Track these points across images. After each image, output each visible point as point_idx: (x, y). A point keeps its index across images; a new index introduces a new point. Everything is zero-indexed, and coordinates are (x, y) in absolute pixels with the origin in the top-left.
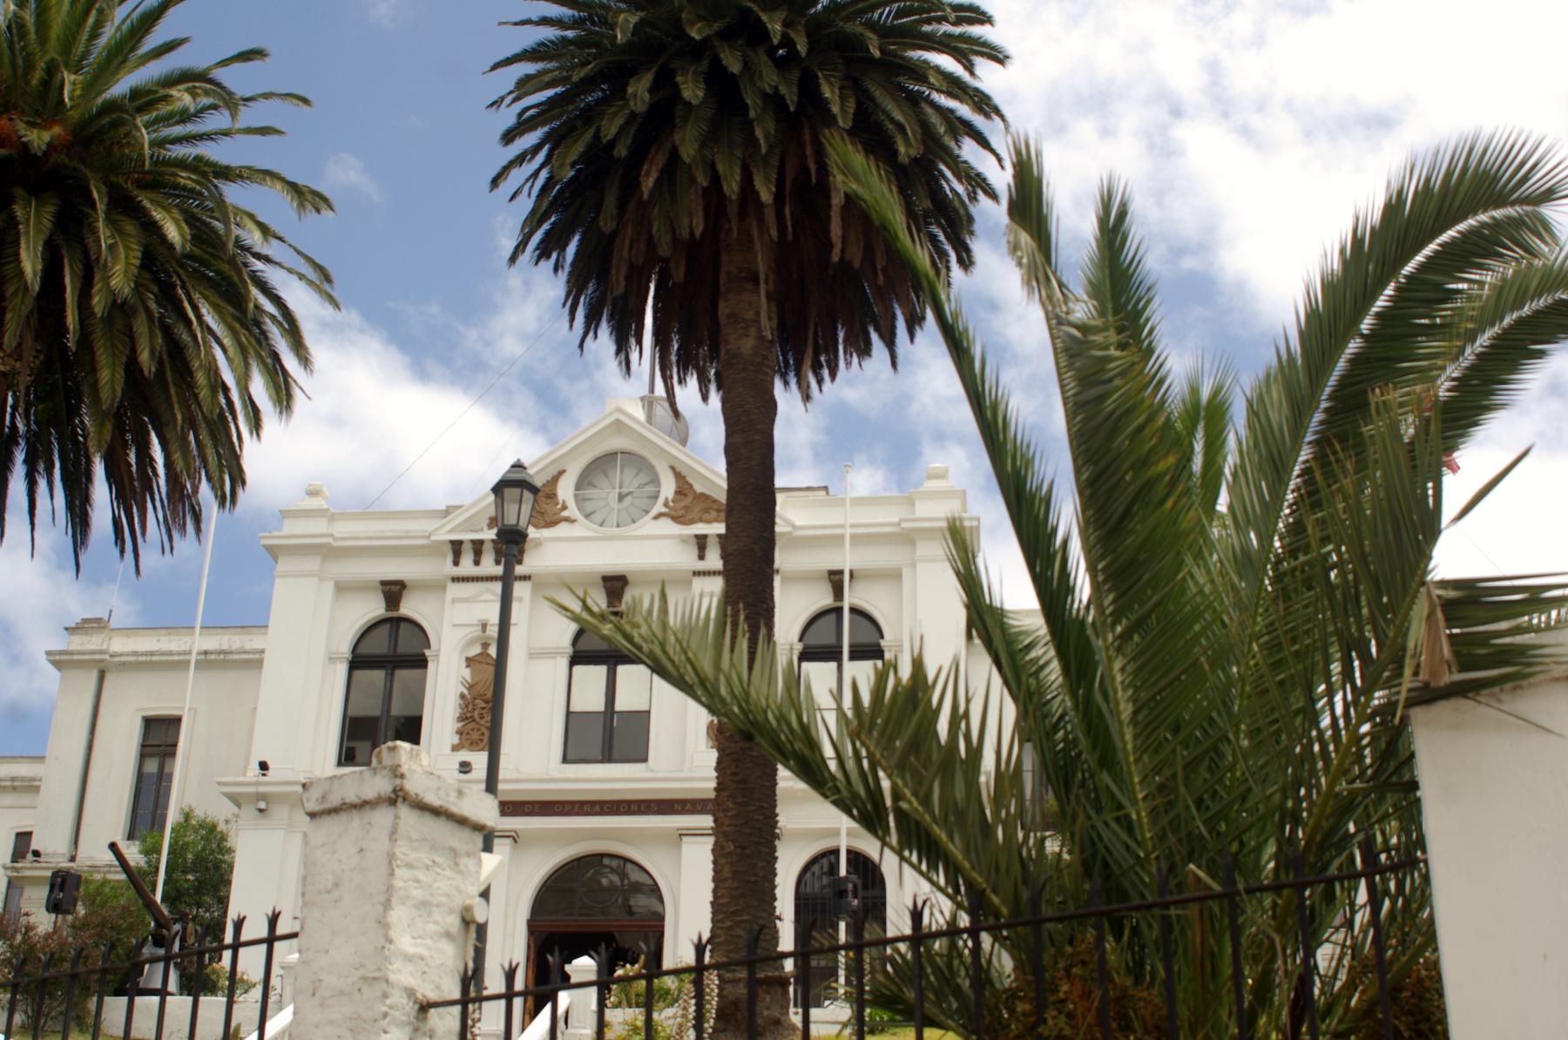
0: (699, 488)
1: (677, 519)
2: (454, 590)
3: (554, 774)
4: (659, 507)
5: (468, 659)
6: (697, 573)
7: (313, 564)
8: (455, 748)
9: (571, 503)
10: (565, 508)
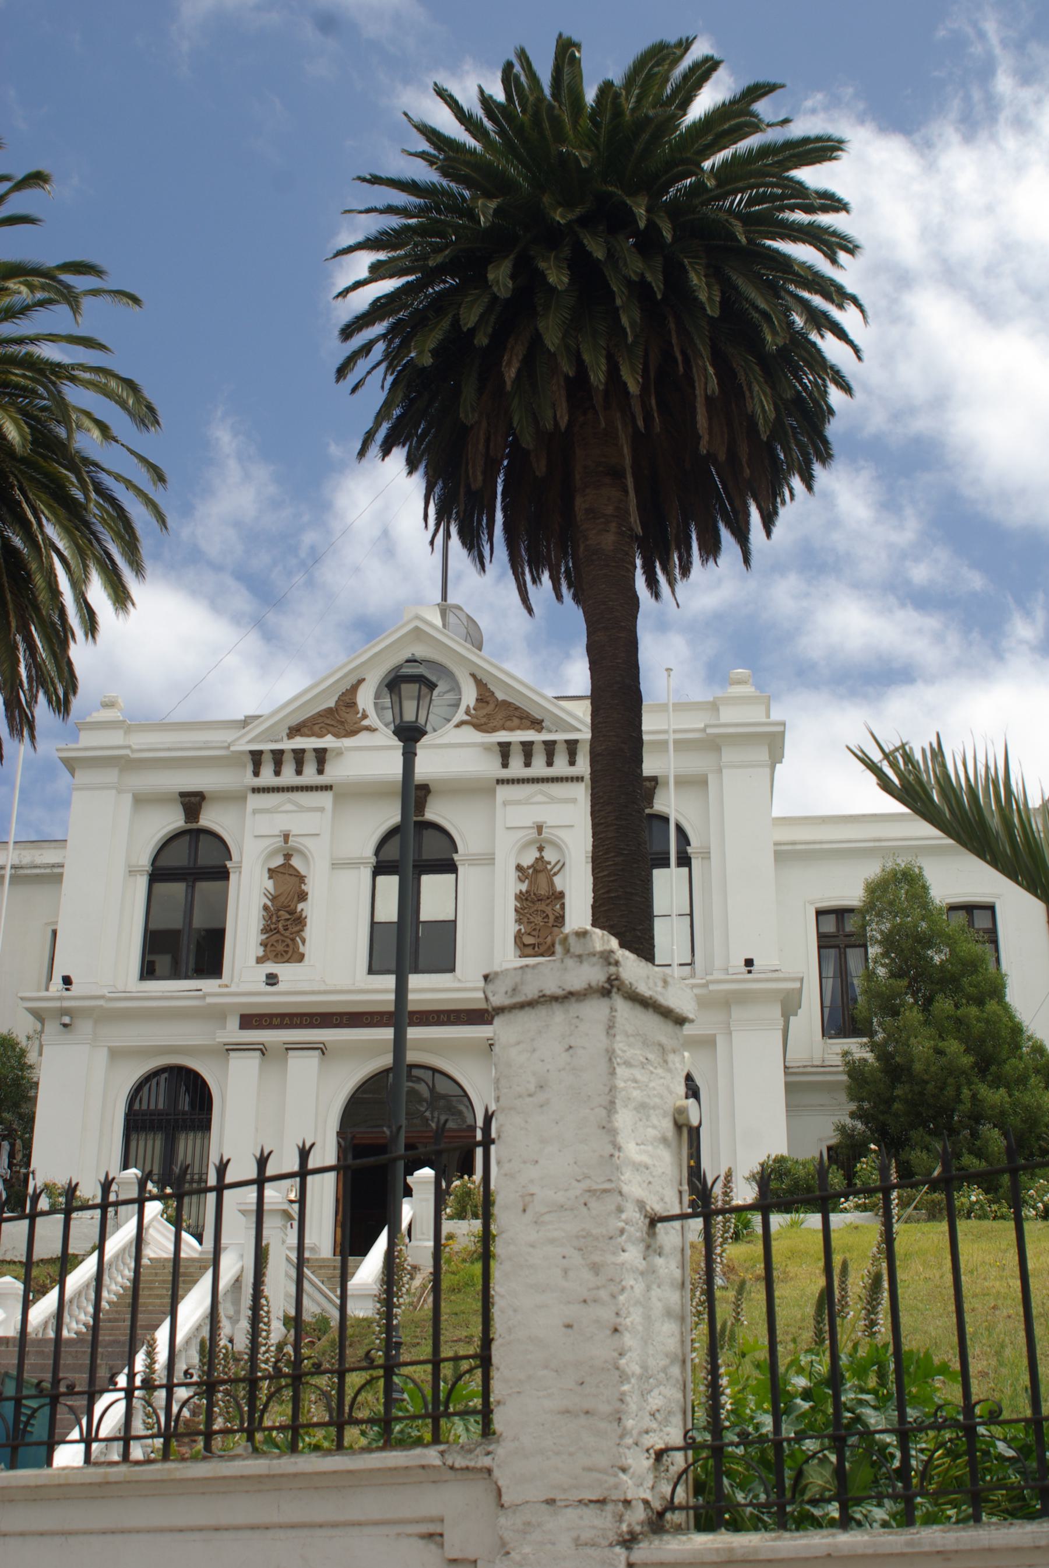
0: (500, 696)
1: (478, 727)
2: (255, 801)
3: (362, 986)
4: (460, 715)
5: (269, 870)
6: (500, 782)
7: (111, 776)
8: (259, 960)
9: (371, 711)
10: (365, 716)
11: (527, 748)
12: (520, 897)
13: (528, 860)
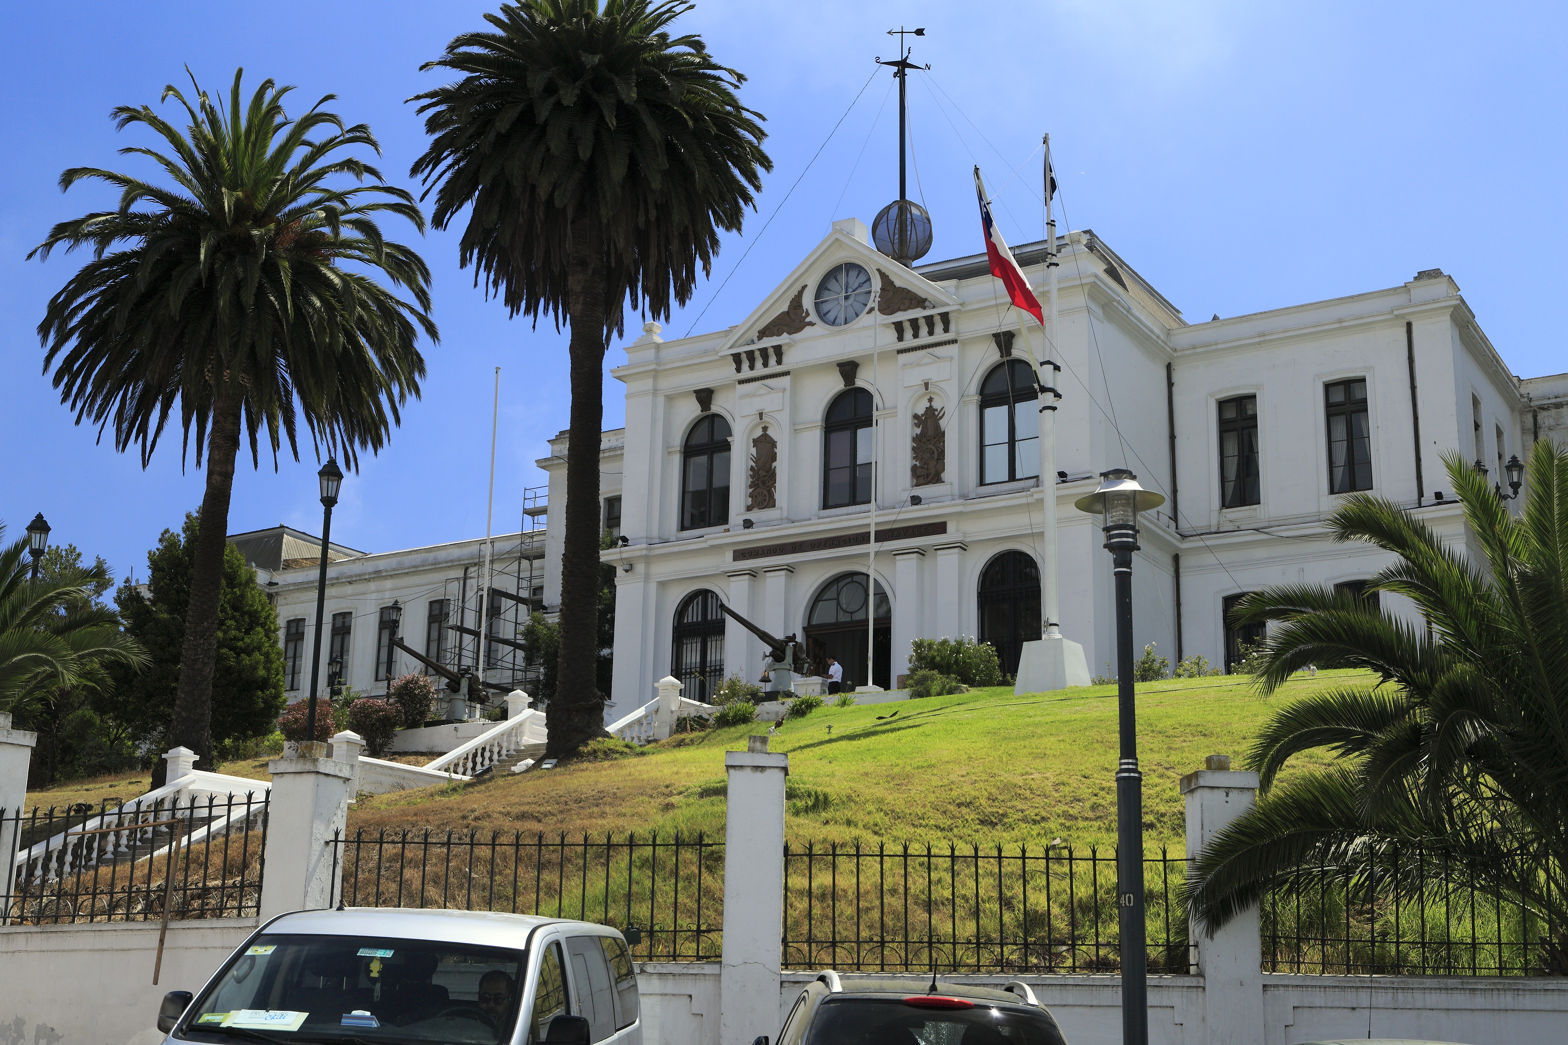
6: (900, 352)
11: (914, 323)
12: (915, 439)
13: (921, 411)
